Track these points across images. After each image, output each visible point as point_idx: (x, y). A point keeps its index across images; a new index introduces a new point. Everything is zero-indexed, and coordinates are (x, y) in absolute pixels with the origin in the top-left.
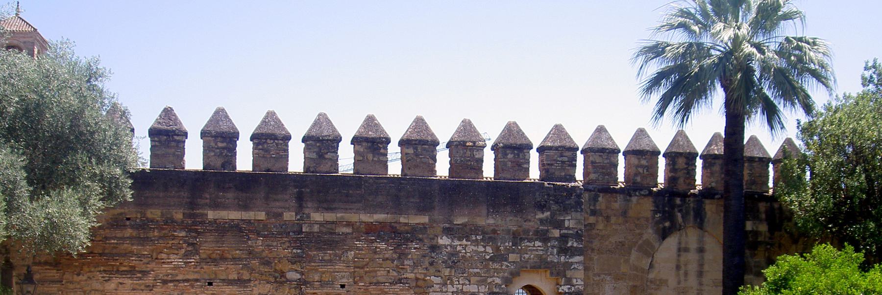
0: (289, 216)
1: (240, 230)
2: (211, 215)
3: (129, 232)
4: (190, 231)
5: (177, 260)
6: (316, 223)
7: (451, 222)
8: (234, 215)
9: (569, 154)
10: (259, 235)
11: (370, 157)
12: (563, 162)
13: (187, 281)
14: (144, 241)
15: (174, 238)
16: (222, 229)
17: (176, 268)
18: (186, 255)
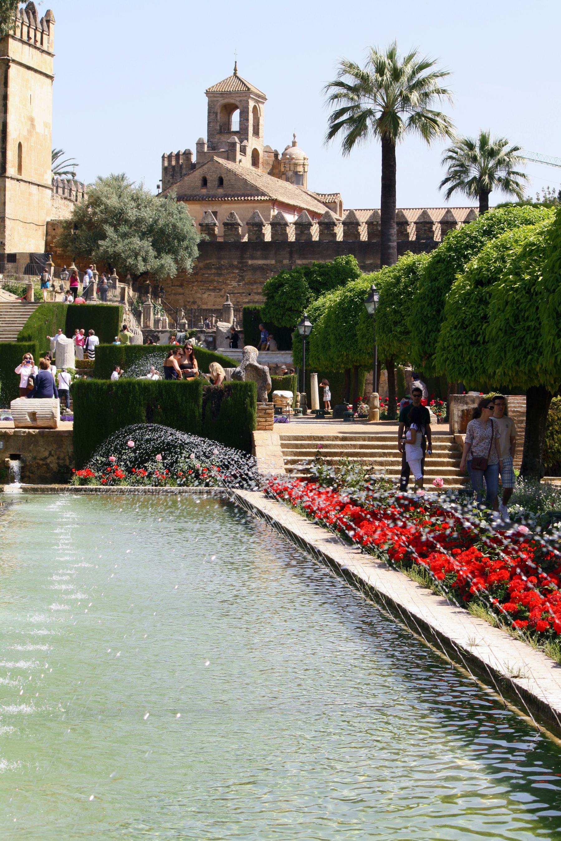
0: (286, 262)
1: (263, 269)
2: (250, 262)
3: (213, 271)
4: (240, 270)
5: (234, 284)
6: (299, 264)
7: (364, 263)
8: (261, 262)
9: (428, 225)
10: (272, 271)
11: (326, 231)
12: (425, 230)
13: (239, 293)
14: (220, 275)
15: (233, 273)
16: (255, 269)
17: (234, 287)
18: (239, 281)
